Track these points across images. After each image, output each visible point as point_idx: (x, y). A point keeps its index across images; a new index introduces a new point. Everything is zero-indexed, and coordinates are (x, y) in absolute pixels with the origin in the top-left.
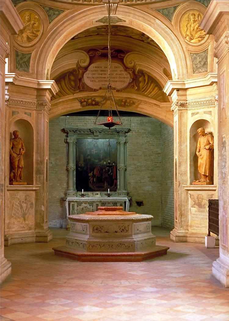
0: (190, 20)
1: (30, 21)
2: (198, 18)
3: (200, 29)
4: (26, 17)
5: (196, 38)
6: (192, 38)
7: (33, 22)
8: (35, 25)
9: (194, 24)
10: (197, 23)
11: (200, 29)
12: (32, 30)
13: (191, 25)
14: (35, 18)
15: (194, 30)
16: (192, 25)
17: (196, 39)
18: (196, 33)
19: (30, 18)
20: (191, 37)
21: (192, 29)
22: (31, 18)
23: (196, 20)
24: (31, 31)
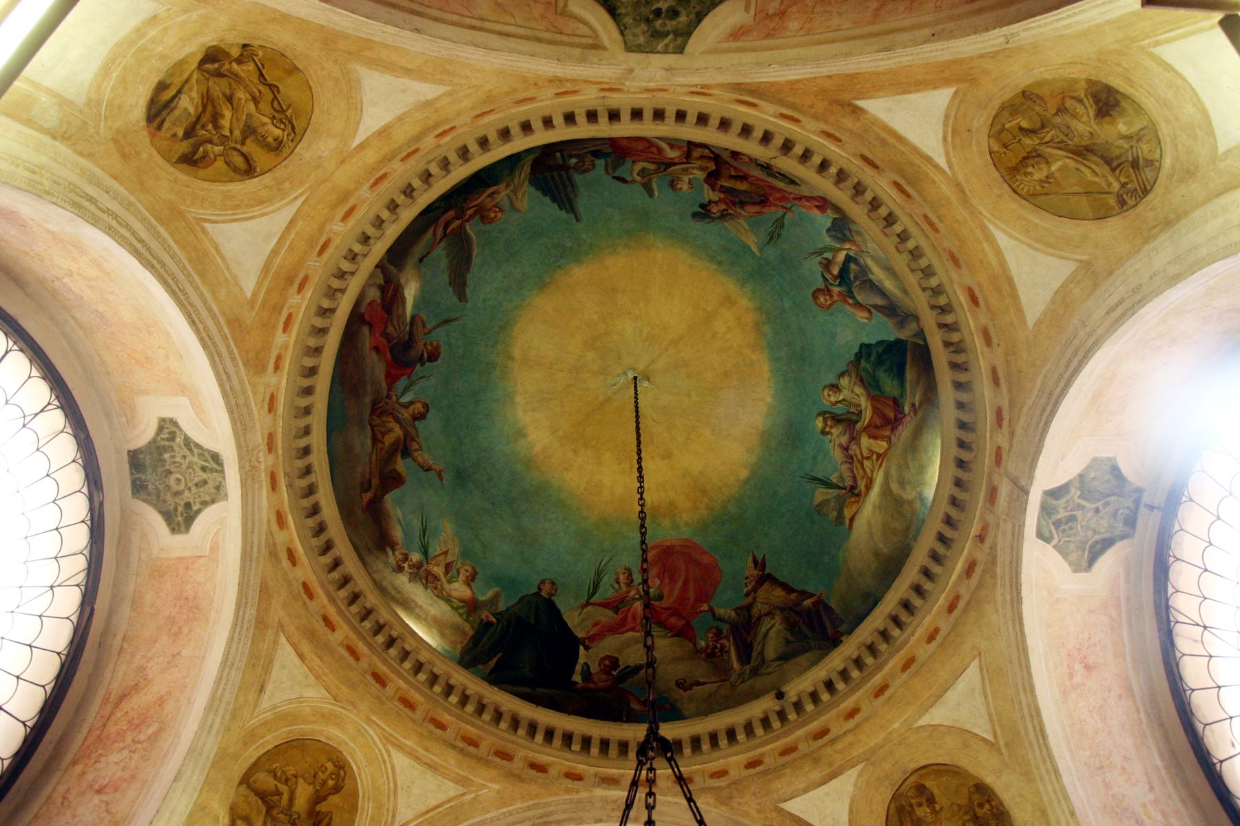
0: (274, 118)
1: (1036, 150)
2: (243, 155)
3: (198, 126)
4: (1041, 181)
5: (187, 81)
6: (208, 66)
7: (1027, 141)
8: (1025, 124)
9: (244, 117)
10: (237, 133)
11: (203, 127)
12: (1057, 120)
13: (256, 101)
14: (1005, 146)
15: (230, 99)
16: (251, 107)
17: (185, 76)
18: (207, 100)
19: (1031, 162)
20: (216, 65)
21: (241, 95)
22: (1025, 158)
23: (248, 142)
24: (1067, 118)
